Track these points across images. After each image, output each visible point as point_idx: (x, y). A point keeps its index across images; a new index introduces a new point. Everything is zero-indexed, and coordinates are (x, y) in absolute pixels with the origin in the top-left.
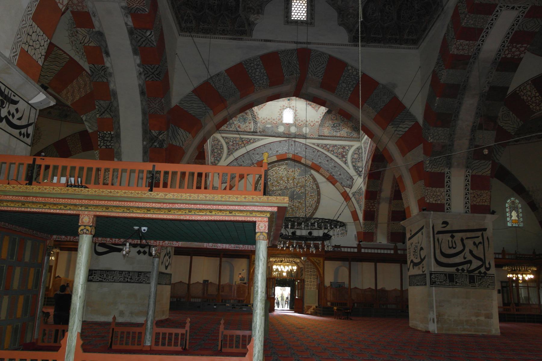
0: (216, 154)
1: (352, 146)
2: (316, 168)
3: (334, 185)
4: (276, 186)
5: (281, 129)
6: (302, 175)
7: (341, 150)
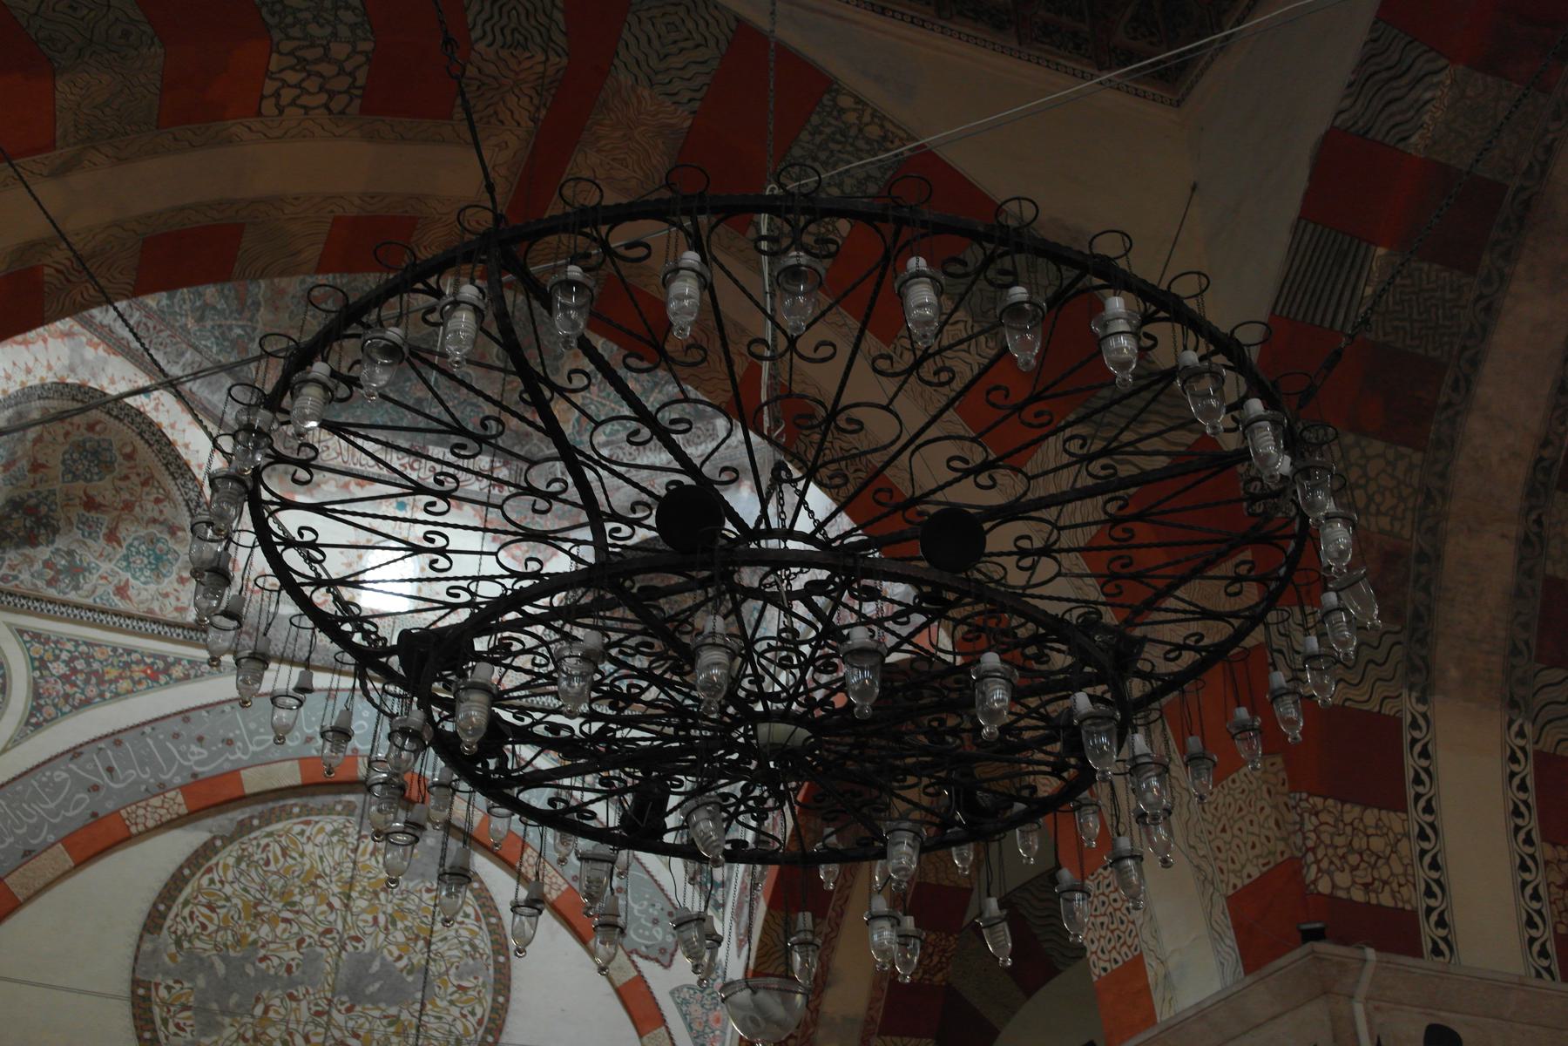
4: (273, 921)
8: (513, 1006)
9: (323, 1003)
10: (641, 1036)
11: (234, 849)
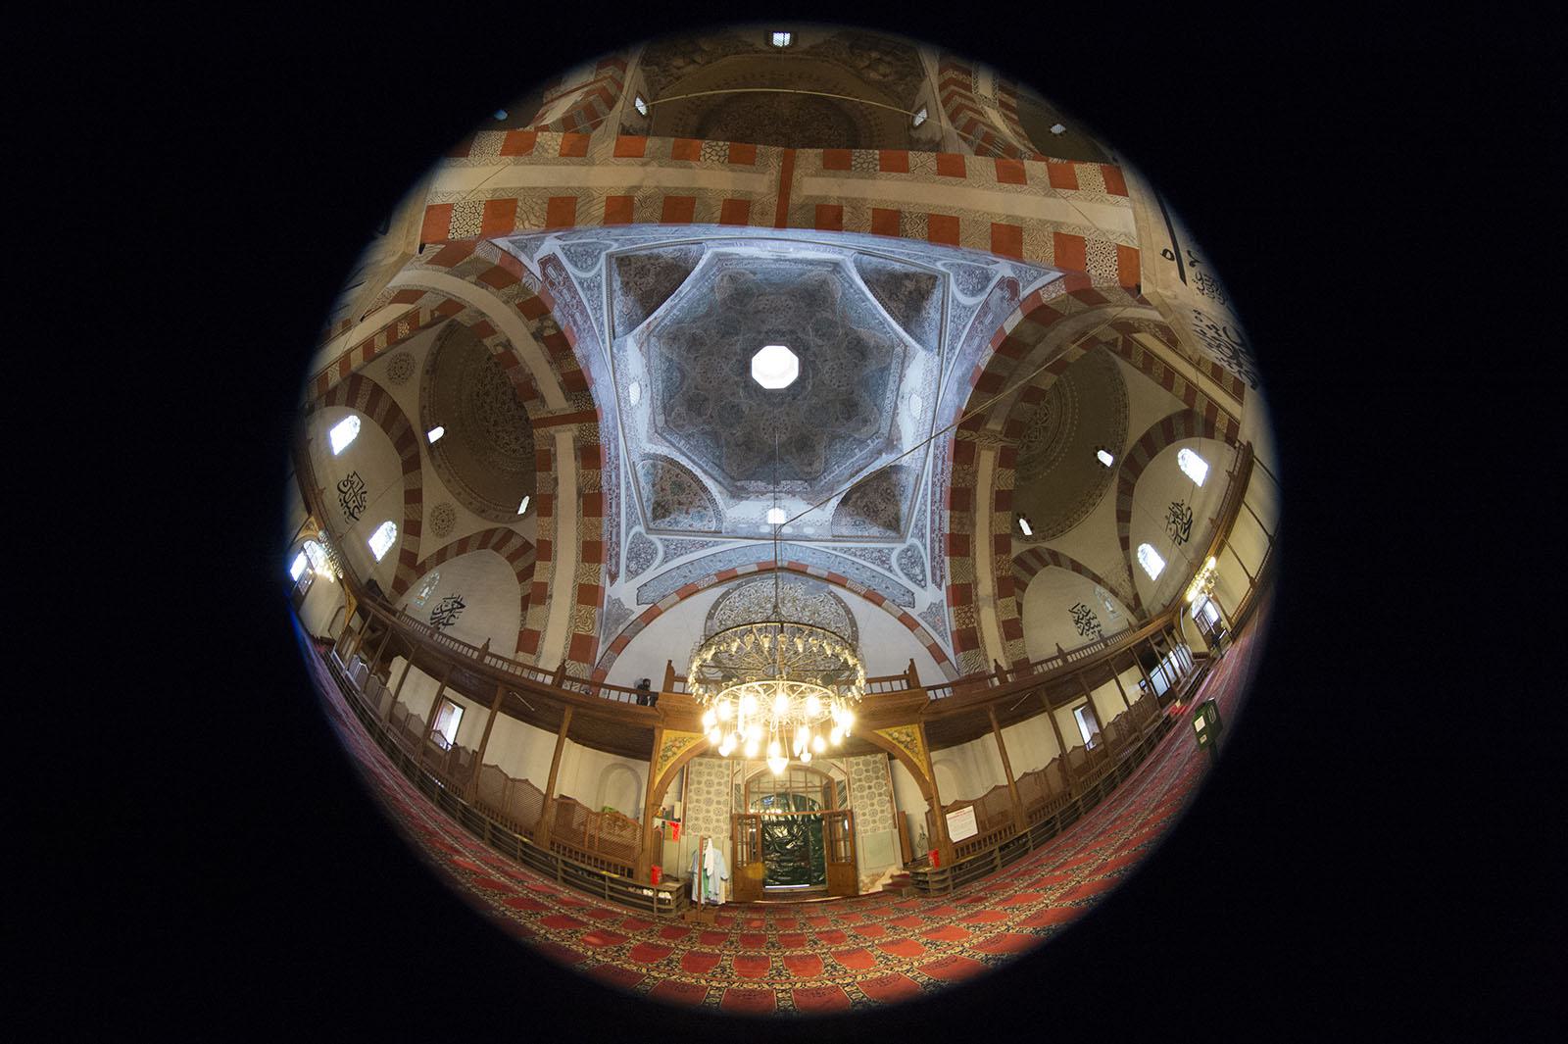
1: (893, 549)
2: (840, 582)
3: (880, 606)
5: (765, 530)
6: (812, 594)
8: (859, 630)
10: (912, 631)
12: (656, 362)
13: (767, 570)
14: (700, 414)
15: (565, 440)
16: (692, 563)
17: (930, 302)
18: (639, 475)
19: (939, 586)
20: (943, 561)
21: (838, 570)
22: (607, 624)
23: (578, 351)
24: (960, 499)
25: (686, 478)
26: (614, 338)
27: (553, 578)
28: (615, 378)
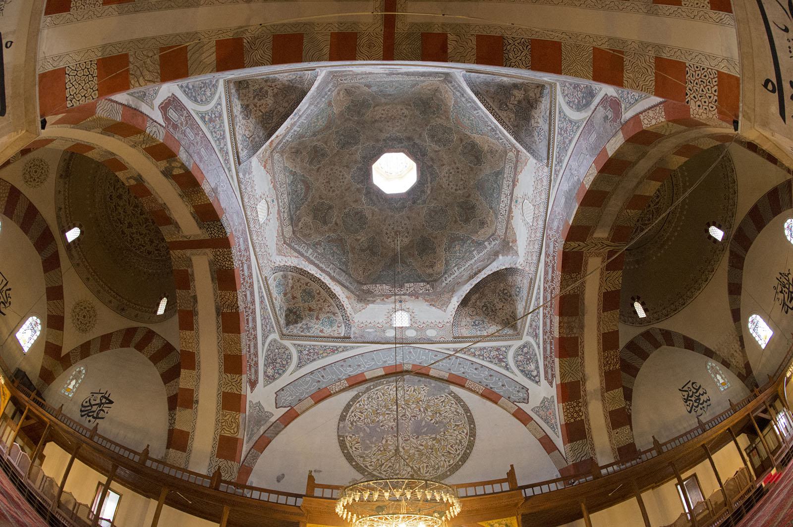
0: (278, 365)
2: (460, 382)
3: (496, 403)
5: (390, 334)
6: (434, 395)
7: (494, 353)
8: (477, 427)
9: (407, 437)
11: (366, 395)
12: (281, 177)
13: (395, 373)
14: (325, 223)
15: (201, 266)
16: (324, 368)
17: (538, 111)
18: (271, 288)
19: (551, 384)
20: (553, 361)
21: (458, 371)
22: (249, 426)
23: (206, 187)
24: (569, 306)
25: (315, 286)
26: (240, 164)
27: (197, 385)
28: (243, 201)
